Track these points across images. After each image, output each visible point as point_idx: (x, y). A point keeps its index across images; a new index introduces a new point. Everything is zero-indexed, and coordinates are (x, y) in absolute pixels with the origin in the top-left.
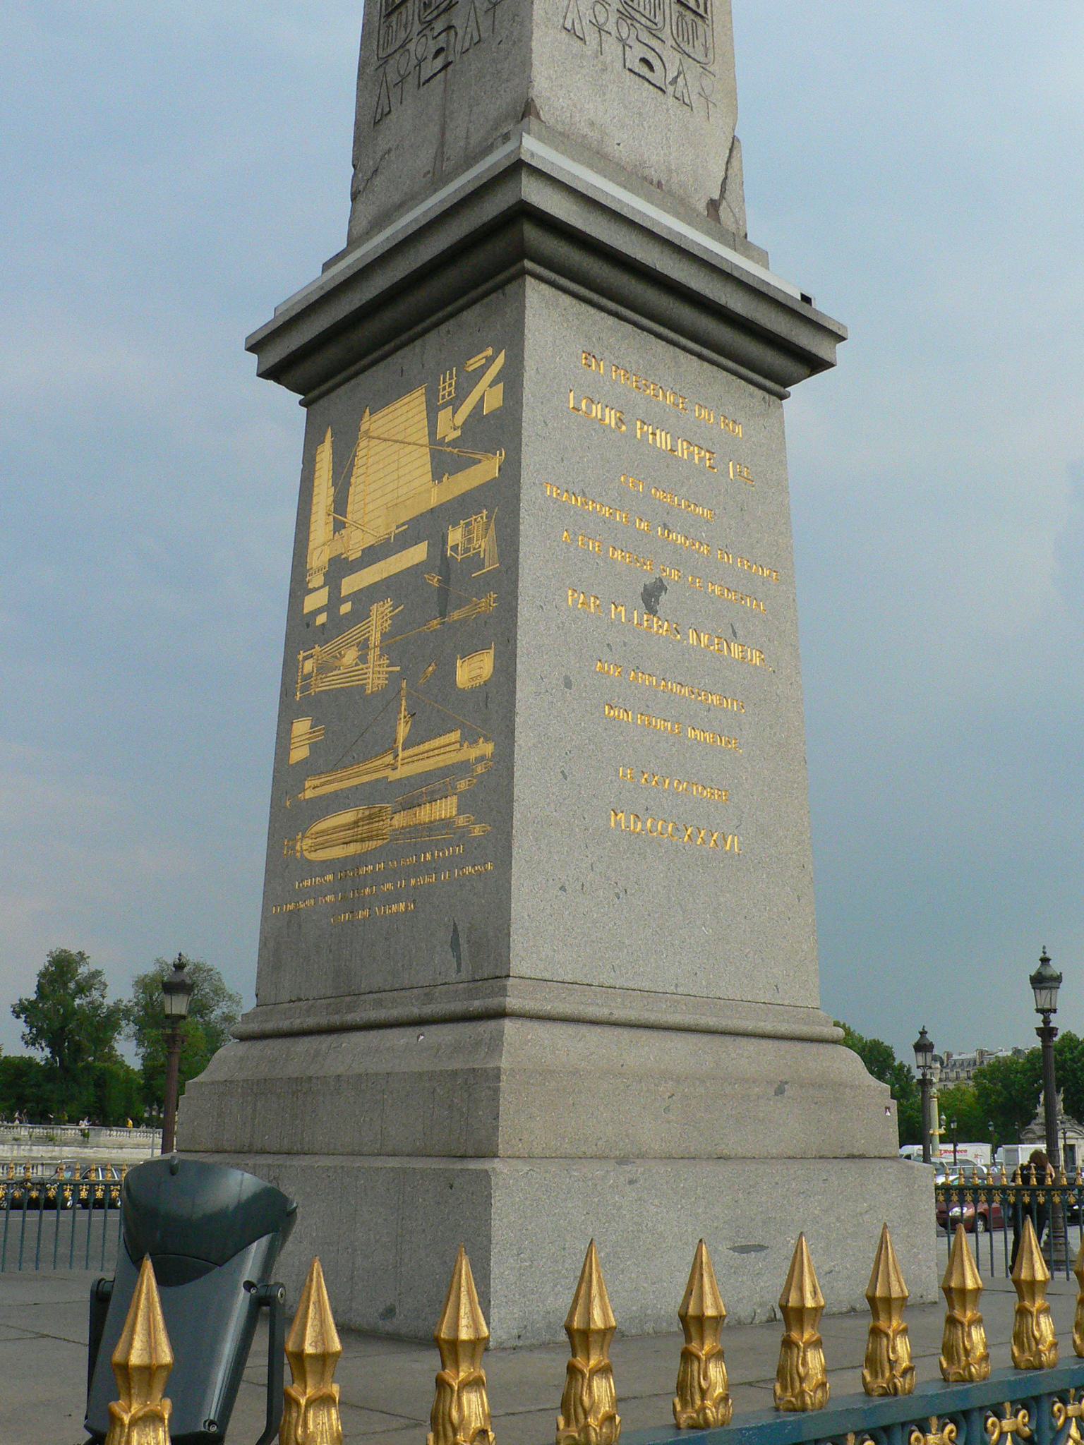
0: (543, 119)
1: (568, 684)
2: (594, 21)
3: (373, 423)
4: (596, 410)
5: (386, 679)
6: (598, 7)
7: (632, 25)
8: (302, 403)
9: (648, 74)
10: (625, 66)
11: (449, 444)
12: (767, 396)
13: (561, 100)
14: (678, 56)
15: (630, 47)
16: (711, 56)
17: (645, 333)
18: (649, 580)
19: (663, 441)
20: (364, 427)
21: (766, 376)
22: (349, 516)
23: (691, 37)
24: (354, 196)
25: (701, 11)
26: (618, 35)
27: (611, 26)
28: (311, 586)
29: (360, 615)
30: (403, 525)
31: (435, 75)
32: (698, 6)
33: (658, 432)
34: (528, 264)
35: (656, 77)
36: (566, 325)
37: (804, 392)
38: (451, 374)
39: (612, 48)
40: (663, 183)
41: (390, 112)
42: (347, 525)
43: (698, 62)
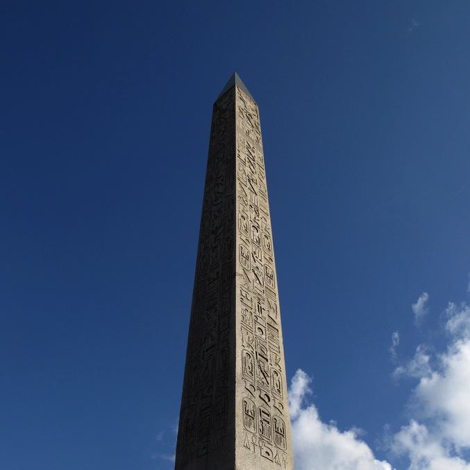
9: (268, 456)
35: (270, 457)
39: (258, 450)
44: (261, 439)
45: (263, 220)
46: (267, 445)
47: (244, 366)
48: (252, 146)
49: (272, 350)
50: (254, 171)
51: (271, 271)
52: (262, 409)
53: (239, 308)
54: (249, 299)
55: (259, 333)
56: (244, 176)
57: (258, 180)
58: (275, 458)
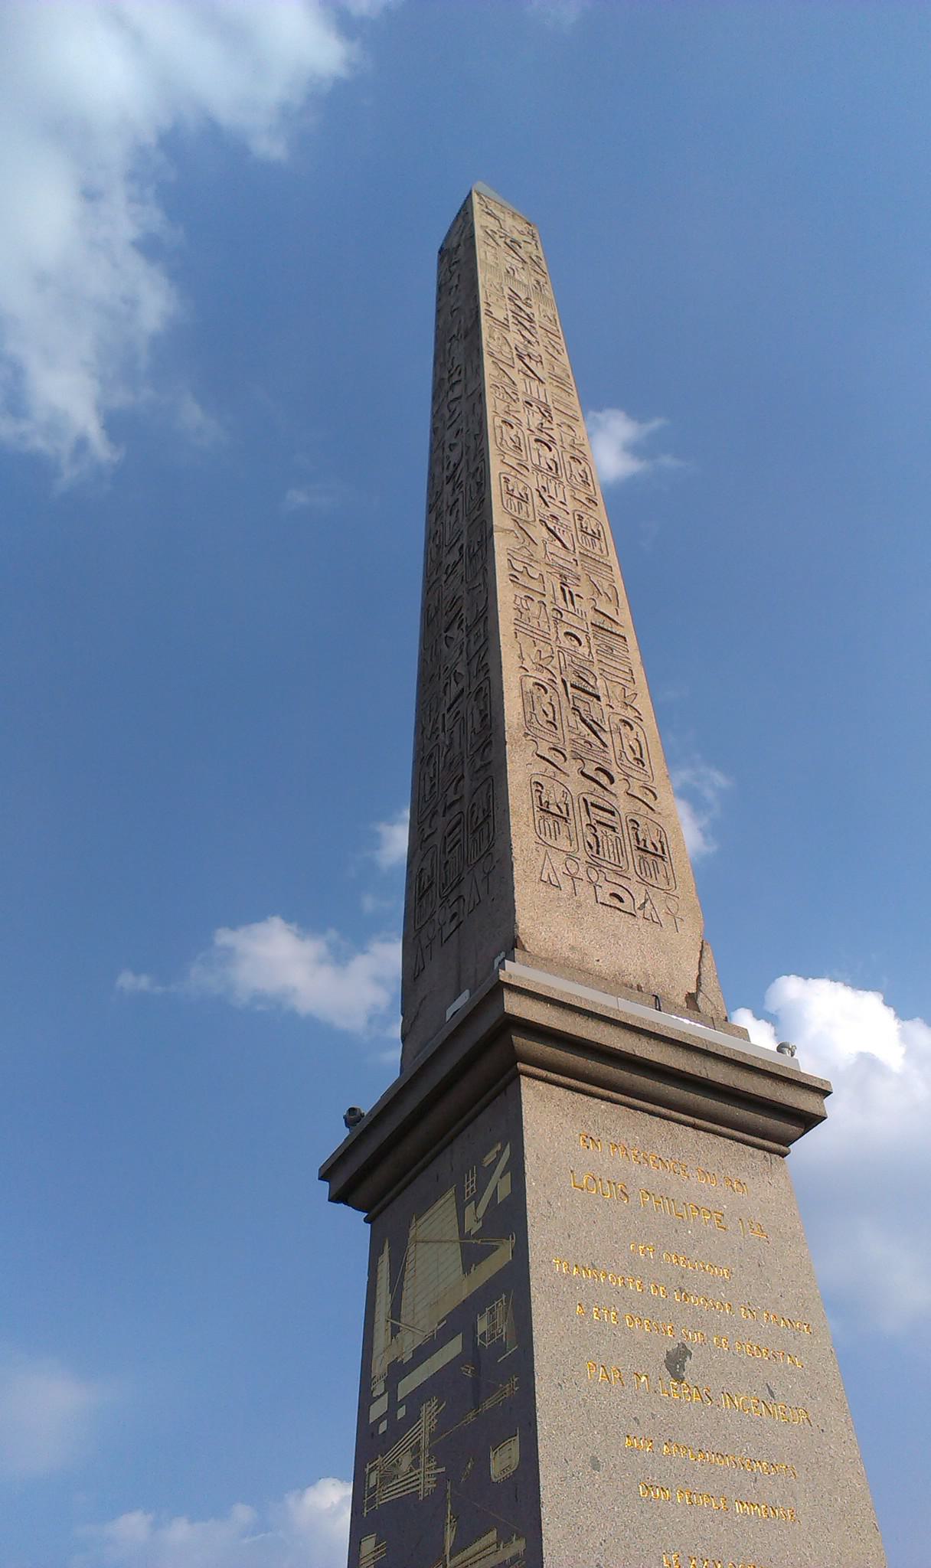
0: (528, 950)
1: (596, 1465)
2: (567, 872)
3: (421, 1228)
5: (435, 1482)
6: (569, 862)
7: (600, 870)
8: (366, 1220)
9: (619, 905)
10: (597, 902)
12: (768, 1155)
13: (543, 933)
14: (644, 887)
15: (601, 887)
16: (672, 882)
17: (639, 1112)
18: (672, 1347)
20: (412, 1233)
22: (402, 1320)
23: (653, 872)
25: (660, 852)
26: (588, 880)
27: (582, 874)
28: (375, 1395)
29: (413, 1418)
30: (443, 1320)
31: (451, 934)
32: (656, 850)
34: (521, 1066)
36: (561, 1114)
38: (473, 1171)
39: (584, 890)
40: (642, 985)
42: (401, 1329)
44: (594, 865)
45: (564, 428)
46: (612, 877)
47: (529, 709)
48: (523, 297)
50: (533, 340)
51: (593, 522)
52: (590, 799)
53: (506, 595)
54: (536, 576)
55: (567, 643)
56: (506, 349)
57: (545, 356)
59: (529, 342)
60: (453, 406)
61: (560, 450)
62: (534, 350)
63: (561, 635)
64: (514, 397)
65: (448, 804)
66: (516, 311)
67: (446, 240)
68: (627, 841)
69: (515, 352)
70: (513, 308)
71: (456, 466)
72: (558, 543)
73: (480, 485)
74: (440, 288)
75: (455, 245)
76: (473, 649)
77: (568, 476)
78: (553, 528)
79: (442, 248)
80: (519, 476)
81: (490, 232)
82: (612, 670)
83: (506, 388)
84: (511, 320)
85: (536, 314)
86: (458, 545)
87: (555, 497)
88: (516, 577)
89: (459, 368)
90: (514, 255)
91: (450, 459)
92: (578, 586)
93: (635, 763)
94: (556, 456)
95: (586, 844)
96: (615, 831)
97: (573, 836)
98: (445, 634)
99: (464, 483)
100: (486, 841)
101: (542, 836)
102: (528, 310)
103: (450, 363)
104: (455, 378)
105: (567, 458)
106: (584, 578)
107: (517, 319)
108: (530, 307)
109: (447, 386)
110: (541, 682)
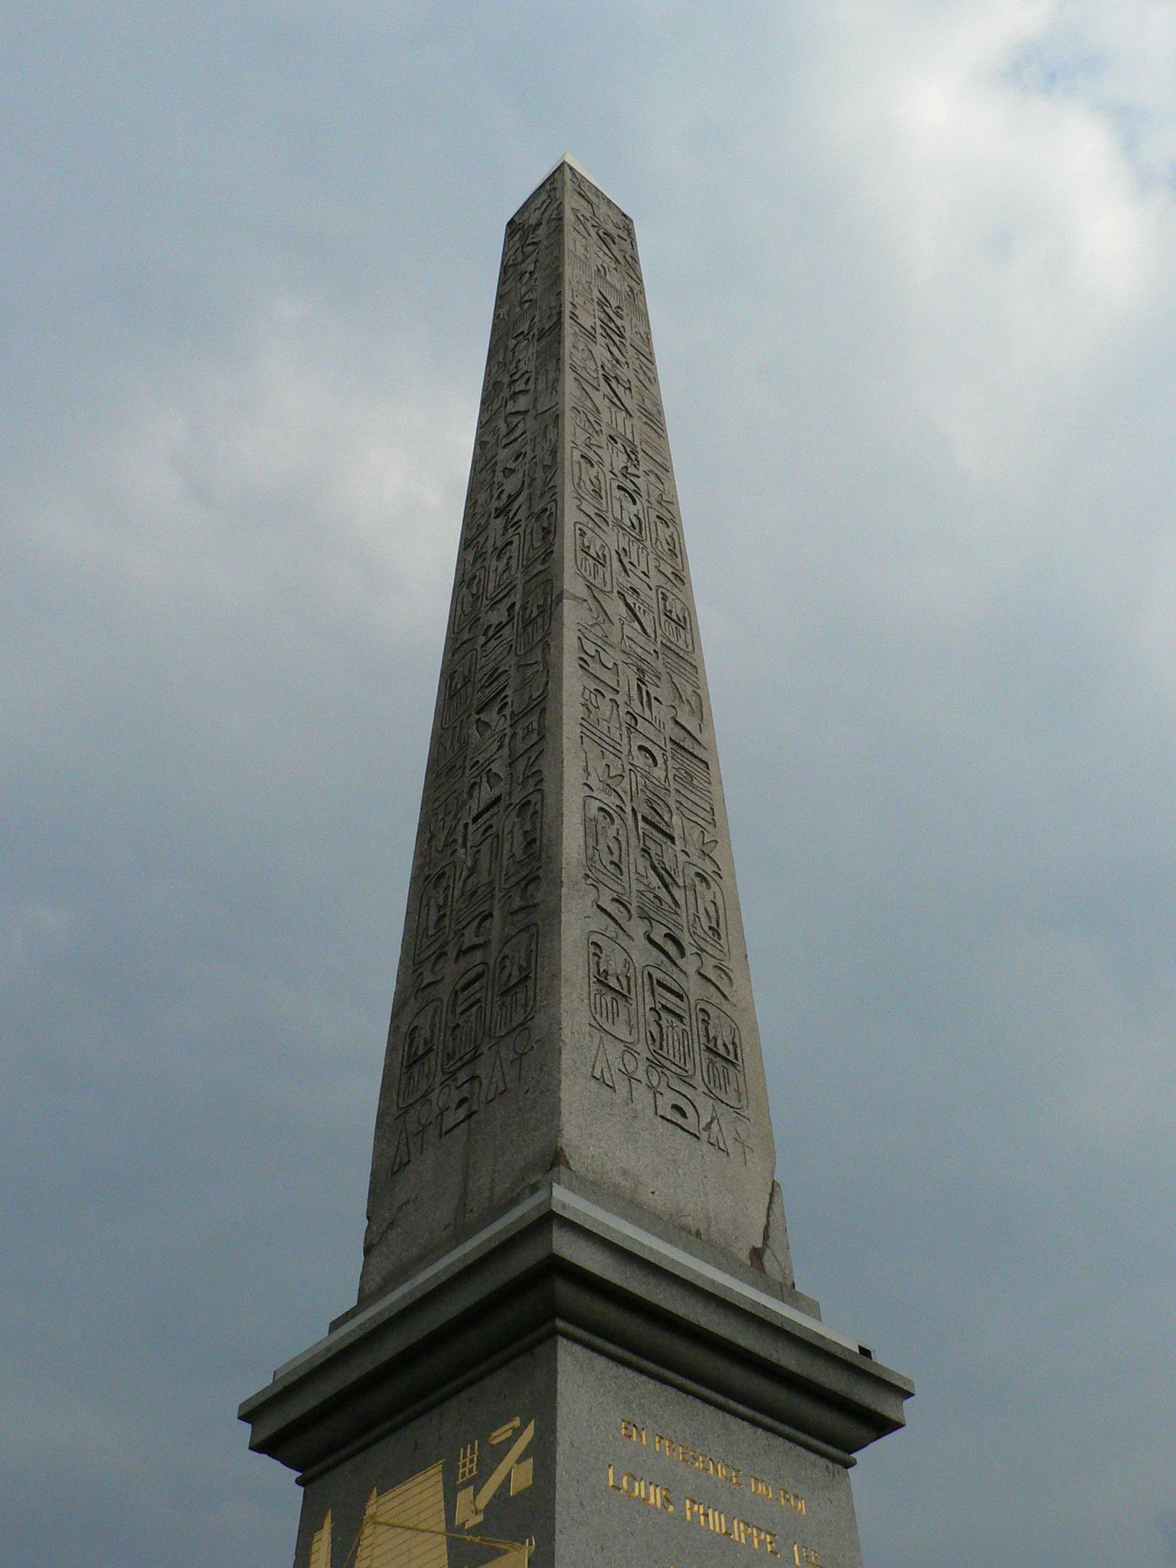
0: (574, 1169)
3: (382, 1506)
4: (639, 1489)
6: (627, 1056)
7: (662, 1072)
8: (298, 1482)
10: (656, 1114)
11: (470, 1532)
12: (830, 1465)
13: (592, 1148)
14: (711, 1101)
15: (661, 1094)
16: (743, 1097)
17: (690, 1397)
19: (716, 1522)
20: (370, 1511)
21: (828, 1442)
23: (722, 1082)
24: (368, 1250)
25: (731, 1057)
26: (648, 1082)
27: (640, 1074)
31: (458, 1124)
32: (728, 1053)
33: (710, 1512)
34: (560, 1324)
35: (690, 1123)
37: (873, 1456)
38: (472, 1449)
39: (642, 1094)
40: (702, 1231)
41: (409, 1161)
43: (733, 1107)
44: (653, 1064)
45: (652, 478)
46: (676, 1084)
47: (591, 843)
48: (614, 304)
49: (687, 813)
50: (622, 360)
51: (679, 606)
52: (657, 975)
53: (572, 684)
54: (610, 666)
55: (640, 760)
56: (591, 365)
58: (709, 1126)
59: (617, 361)
60: (515, 420)
61: (646, 505)
62: (625, 373)
63: (635, 748)
64: (598, 428)
65: (464, 948)
66: (606, 321)
67: (520, 212)
68: (695, 1037)
69: (601, 372)
70: (602, 316)
71: (512, 499)
72: (636, 625)
73: (546, 532)
74: (505, 269)
75: (533, 221)
76: (521, 747)
77: (654, 540)
78: (632, 606)
79: (512, 220)
80: (597, 530)
81: (582, 219)
82: (689, 805)
83: (588, 414)
84: (599, 330)
85: (628, 328)
86: (507, 602)
87: (636, 564)
88: (587, 663)
89: (526, 376)
90: (607, 251)
91: (504, 487)
92: (658, 686)
93: (710, 933)
94: (641, 512)
95: (648, 1034)
96: (682, 1022)
97: (633, 1022)
98: (477, 717)
99: (523, 523)
100: (521, 1010)
101: (598, 1017)
102: (619, 322)
103: (514, 365)
104: (520, 386)
105: (653, 517)
106: (665, 676)
107: (605, 331)
108: (621, 318)
109: (506, 393)
110: (608, 809)
